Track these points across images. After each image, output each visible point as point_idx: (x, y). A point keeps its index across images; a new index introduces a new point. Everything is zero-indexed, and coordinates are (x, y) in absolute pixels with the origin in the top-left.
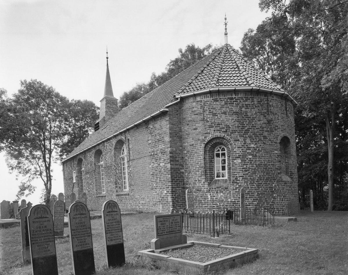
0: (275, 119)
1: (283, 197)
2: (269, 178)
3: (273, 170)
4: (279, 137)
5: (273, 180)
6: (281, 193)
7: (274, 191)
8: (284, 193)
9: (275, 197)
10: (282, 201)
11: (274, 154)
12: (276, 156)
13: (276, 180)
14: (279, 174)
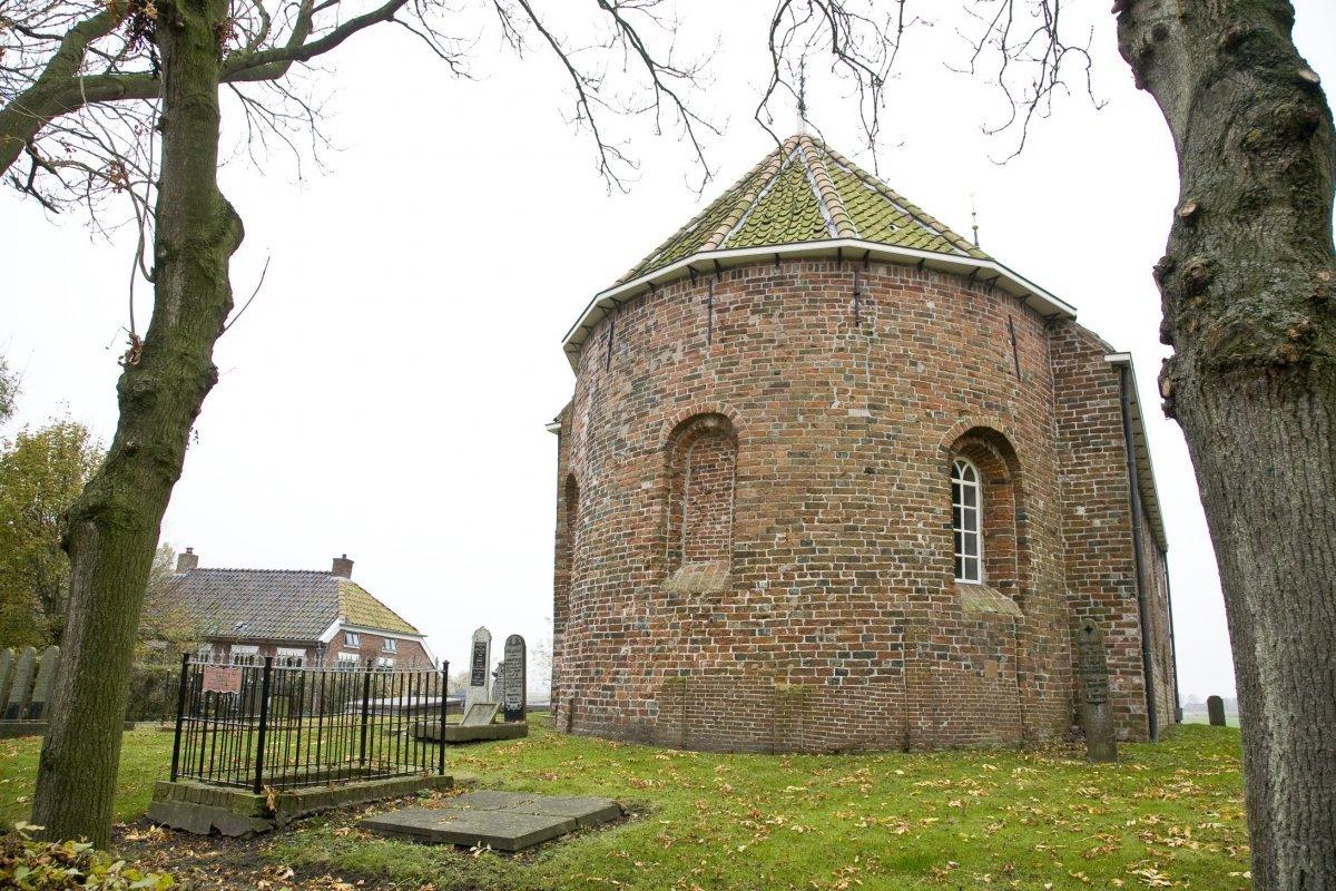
0: (658, 368)
1: (656, 658)
2: (611, 587)
3: (630, 555)
4: (666, 425)
5: (624, 592)
6: (647, 642)
7: (622, 635)
8: (659, 642)
9: (625, 658)
10: (648, 673)
11: (638, 494)
12: (646, 502)
13: (632, 591)
14: (647, 568)
